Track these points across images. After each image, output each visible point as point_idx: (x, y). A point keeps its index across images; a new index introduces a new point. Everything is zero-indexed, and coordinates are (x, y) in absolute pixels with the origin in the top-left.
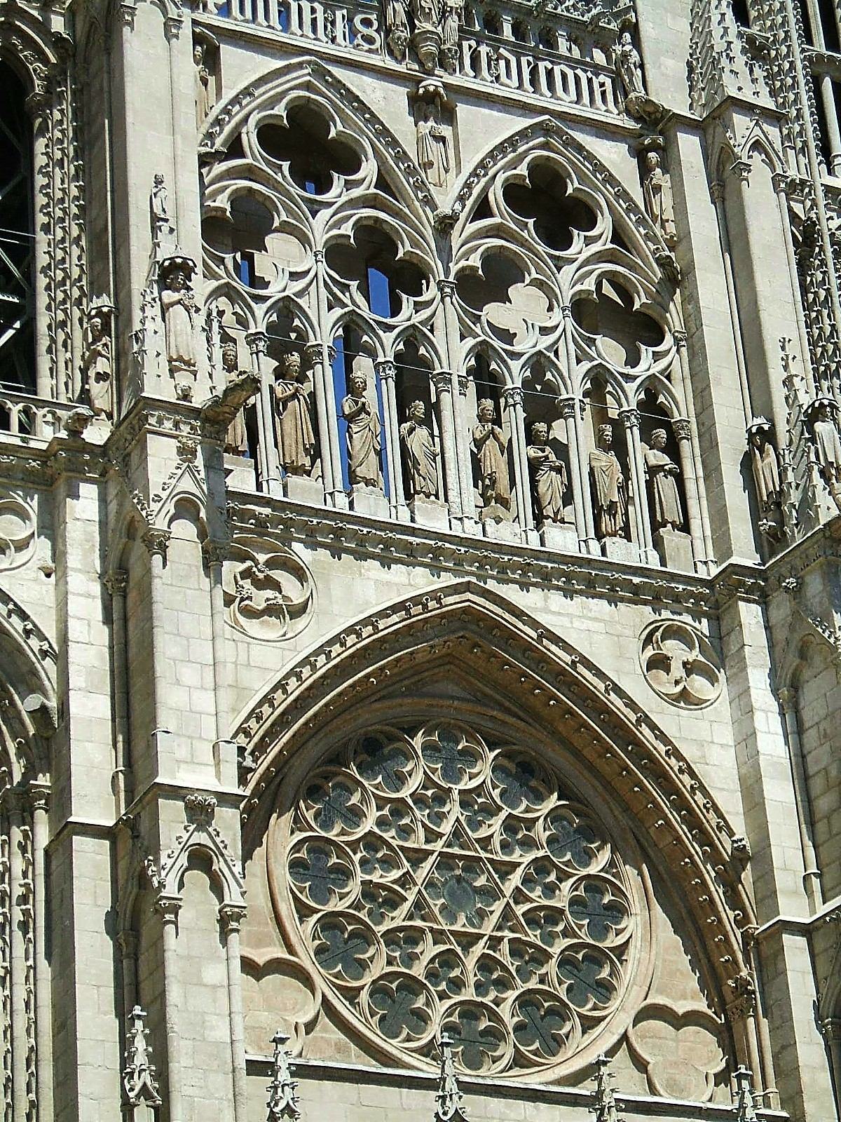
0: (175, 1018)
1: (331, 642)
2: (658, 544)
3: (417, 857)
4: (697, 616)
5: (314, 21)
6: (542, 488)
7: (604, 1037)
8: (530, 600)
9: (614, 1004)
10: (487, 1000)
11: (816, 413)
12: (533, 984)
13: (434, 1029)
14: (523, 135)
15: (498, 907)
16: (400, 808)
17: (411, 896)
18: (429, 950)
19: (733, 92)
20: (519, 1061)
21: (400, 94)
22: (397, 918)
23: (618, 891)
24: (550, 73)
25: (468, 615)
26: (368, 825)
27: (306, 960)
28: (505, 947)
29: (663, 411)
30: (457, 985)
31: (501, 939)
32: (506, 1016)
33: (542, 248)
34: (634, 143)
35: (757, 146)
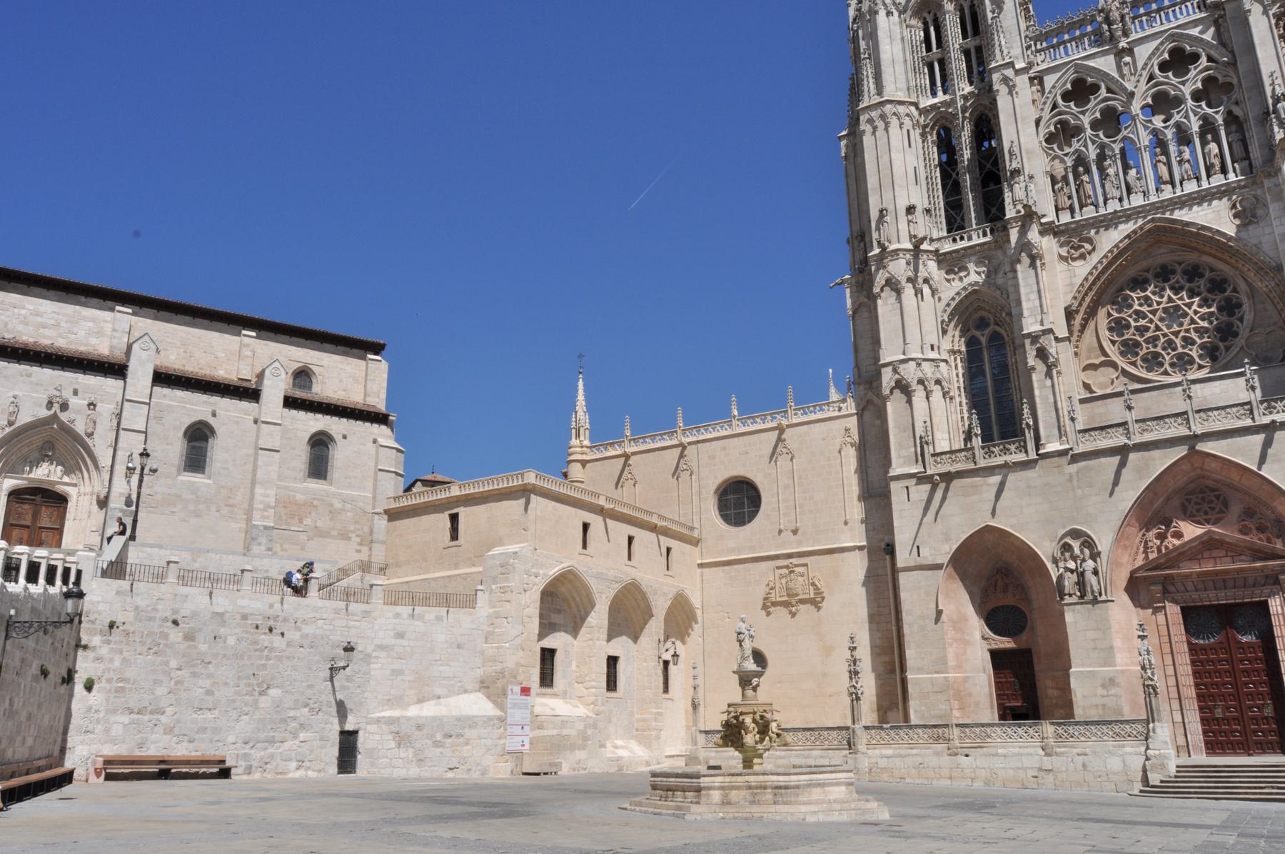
0: (1038, 400)
1: (1102, 258)
3: (1154, 312)
7: (1234, 351)
8: (1181, 215)
13: (1167, 366)
14: (1162, 43)
15: (1186, 321)
17: (1152, 326)
18: (1162, 340)
23: (1237, 298)
26: (1136, 307)
27: (1115, 359)
29: (1237, 117)
31: (1190, 329)
32: (1194, 354)
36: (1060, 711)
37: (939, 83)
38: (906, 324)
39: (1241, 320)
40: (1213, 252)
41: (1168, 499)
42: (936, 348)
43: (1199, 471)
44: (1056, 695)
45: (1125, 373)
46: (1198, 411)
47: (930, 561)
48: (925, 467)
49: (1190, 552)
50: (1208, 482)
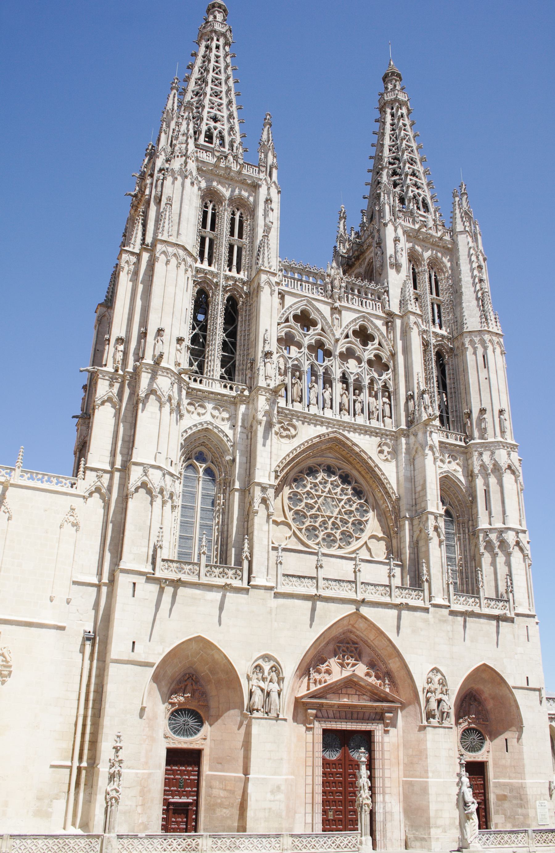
0: (255, 539)
1: (301, 445)
2: (383, 421)
3: (319, 497)
4: (391, 439)
5: (309, 289)
6: (356, 407)
9: (364, 534)
10: (333, 532)
11: (424, 392)
12: (345, 529)
14: (358, 318)
15: (338, 509)
16: (315, 485)
17: (317, 506)
18: (320, 519)
19: (410, 309)
20: (340, 547)
21: (328, 308)
22: (313, 512)
24: (366, 302)
25: (335, 439)
26: (308, 488)
27: (290, 521)
28: (339, 519)
30: (326, 528)
31: (337, 518)
33: (361, 347)
34: (385, 320)
35: (415, 323)
36: (225, 810)
37: (206, 255)
38: (161, 435)
39: (367, 521)
40: (360, 469)
41: (328, 643)
42: (173, 464)
43: (350, 627)
44: (222, 795)
45: (294, 533)
46: (362, 583)
47: (142, 659)
48: (154, 569)
49: (336, 687)
50: (353, 636)
